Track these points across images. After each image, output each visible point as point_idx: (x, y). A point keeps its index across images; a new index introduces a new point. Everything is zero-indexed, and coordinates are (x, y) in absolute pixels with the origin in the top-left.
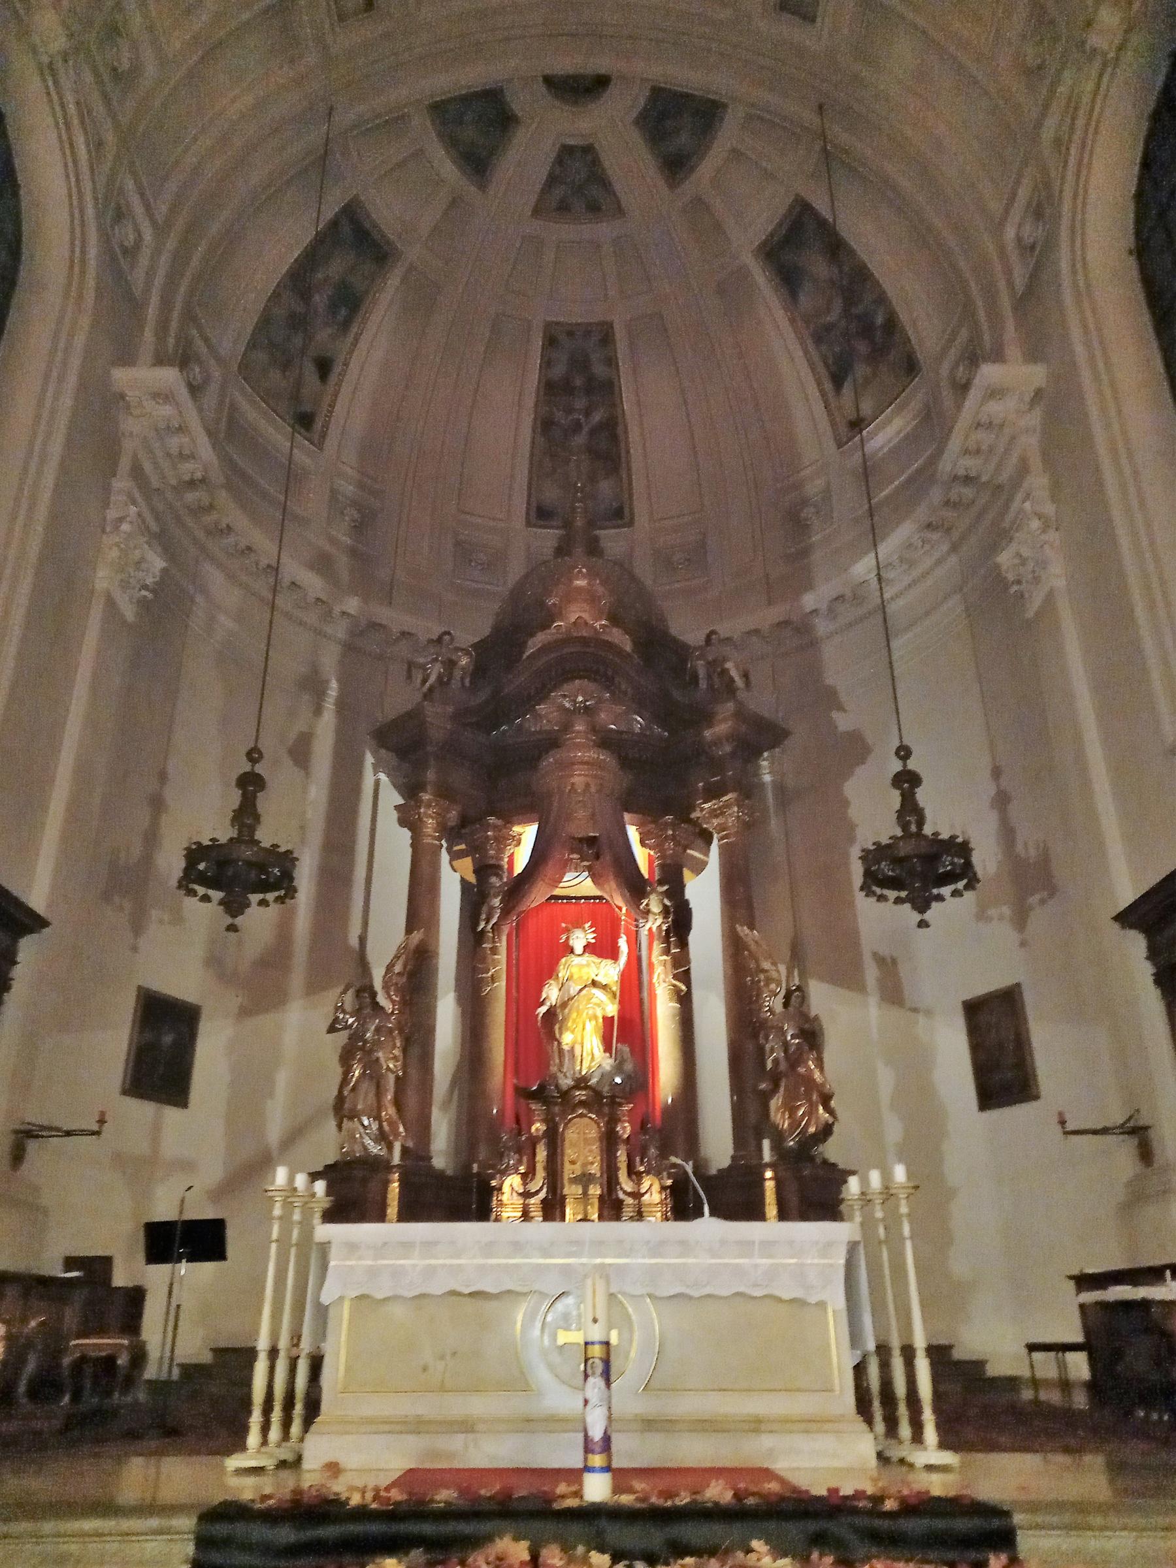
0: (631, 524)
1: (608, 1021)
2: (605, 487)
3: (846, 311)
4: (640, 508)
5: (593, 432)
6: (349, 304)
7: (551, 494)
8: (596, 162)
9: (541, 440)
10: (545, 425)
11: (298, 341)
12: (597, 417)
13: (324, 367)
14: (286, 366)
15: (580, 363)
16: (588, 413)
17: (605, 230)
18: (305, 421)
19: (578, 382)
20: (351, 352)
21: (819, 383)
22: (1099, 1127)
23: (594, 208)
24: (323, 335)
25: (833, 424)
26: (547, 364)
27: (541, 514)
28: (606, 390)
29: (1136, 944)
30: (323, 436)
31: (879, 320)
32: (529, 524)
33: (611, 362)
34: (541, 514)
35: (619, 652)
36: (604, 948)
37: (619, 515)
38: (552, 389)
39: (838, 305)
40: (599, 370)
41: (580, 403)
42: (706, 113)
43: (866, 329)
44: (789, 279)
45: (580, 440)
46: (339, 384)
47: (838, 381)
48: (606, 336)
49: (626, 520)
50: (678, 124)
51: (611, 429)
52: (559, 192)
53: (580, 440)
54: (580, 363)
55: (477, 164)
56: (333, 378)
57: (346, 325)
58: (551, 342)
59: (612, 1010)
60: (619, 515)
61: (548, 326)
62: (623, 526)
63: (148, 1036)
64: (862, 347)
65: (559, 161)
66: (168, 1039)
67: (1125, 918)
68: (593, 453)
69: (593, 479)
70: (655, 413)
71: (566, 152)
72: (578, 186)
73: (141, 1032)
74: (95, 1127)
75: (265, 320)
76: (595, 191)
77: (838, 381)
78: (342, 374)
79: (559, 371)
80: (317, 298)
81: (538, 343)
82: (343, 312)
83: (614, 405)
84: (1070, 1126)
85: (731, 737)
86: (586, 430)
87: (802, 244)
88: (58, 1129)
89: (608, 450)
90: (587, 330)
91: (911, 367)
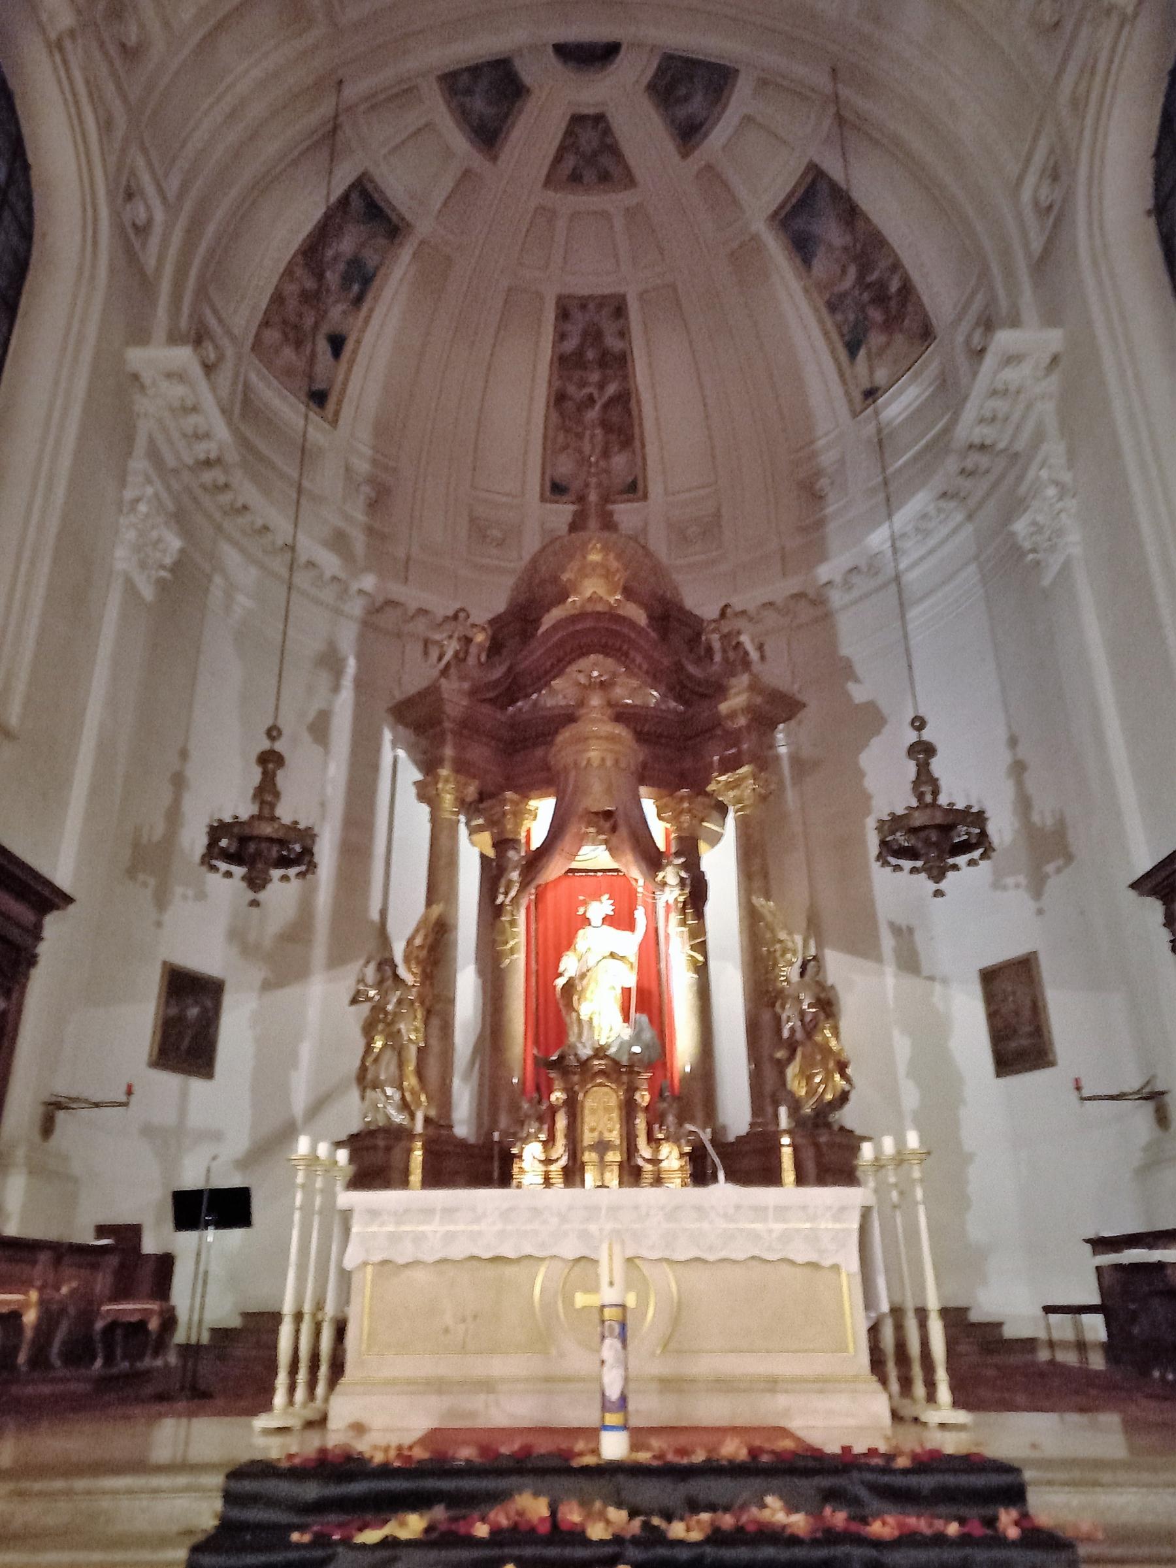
0: (645, 497)
1: (626, 992)
2: (619, 461)
3: (861, 276)
5: (606, 406)
6: (361, 280)
7: (565, 467)
8: (607, 131)
9: (554, 416)
10: (559, 398)
12: (612, 389)
13: (337, 343)
14: (298, 344)
15: (593, 335)
16: (601, 386)
18: (319, 398)
19: (590, 354)
20: (363, 330)
21: (833, 351)
22: (1114, 1092)
23: (605, 177)
24: (336, 311)
25: (847, 393)
26: (561, 336)
27: (557, 489)
28: (618, 363)
29: (1154, 910)
30: (337, 413)
31: (894, 286)
32: (543, 499)
33: (623, 334)
34: (557, 489)
35: (632, 624)
36: (622, 920)
37: (634, 489)
38: (566, 363)
39: (852, 271)
40: (613, 343)
42: (717, 79)
43: (881, 298)
44: (803, 247)
45: (593, 414)
46: (352, 362)
47: (853, 348)
48: (619, 310)
49: (640, 493)
50: (690, 89)
51: (624, 400)
52: (570, 161)
53: (593, 414)
54: (593, 335)
55: (488, 136)
57: (358, 300)
58: (563, 314)
59: (631, 981)
60: (634, 489)
63: (173, 1011)
64: (876, 315)
65: (569, 133)
66: (193, 1012)
67: (1144, 885)
68: (605, 425)
69: (606, 454)
70: (666, 385)
71: (577, 120)
72: (591, 154)
73: (167, 1004)
74: (123, 1099)
75: (278, 298)
76: (606, 160)
77: (853, 348)
78: (355, 352)
79: (570, 345)
80: (328, 274)
81: (550, 315)
82: (356, 288)
84: (1086, 1093)
85: (749, 709)
86: (598, 407)
87: (815, 210)
88: (86, 1101)
89: (621, 424)
90: (602, 301)
91: (926, 334)
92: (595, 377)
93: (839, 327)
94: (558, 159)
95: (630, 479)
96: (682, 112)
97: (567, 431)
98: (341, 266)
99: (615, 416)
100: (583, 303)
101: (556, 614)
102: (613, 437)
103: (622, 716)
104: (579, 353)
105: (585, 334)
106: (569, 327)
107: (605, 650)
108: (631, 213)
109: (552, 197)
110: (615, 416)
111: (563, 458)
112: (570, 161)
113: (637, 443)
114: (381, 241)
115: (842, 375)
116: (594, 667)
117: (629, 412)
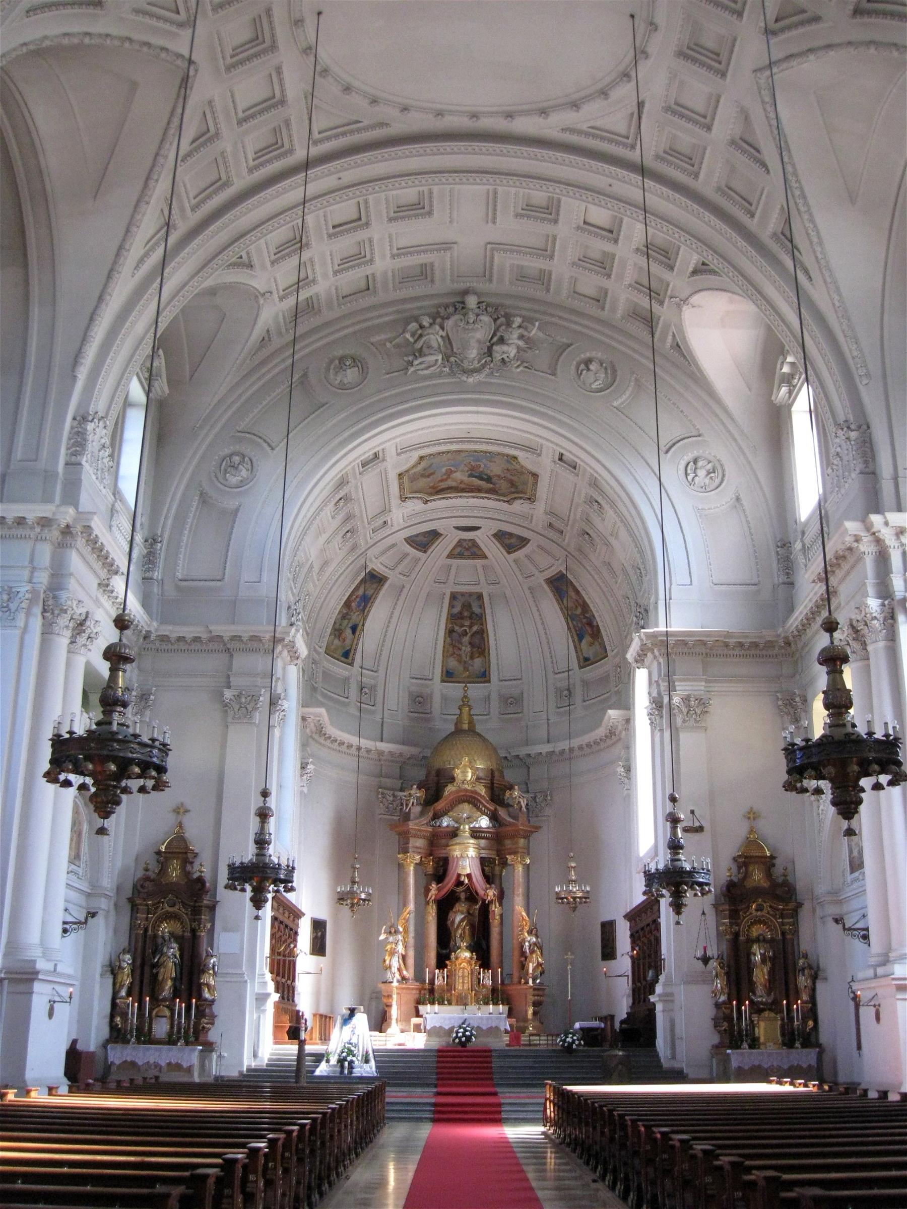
0: (489, 681)
2: (478, 662)
4: (494, 677)
5: (472, 635)
7: (453, 663)
10: (450, 632)
11: (346, 622)
12: (475, 628)
13: (354, 629)
15: (467, 606)
16: (470, 627)
17: (479, 562)
18: (347, 656)
19: (466, 614)
24: (355, 617)
25: (578, 657)
26: (451, 606)
27: (448, 676)
30: (353, 659)
32: (443, 681)
33: (482, 606)
34: (448, 676)
37: (484, 676)
38: (454, 618)
40: (477, 610)
43: (590, 624)
45: (466, 639)
47: (581, 637)
48: (480, 596)
50: (510, 542)
51: (482, 633)
53: (466, 639)
54: (467, 606)
56: (357, 633)
58: (454, 597)
60: (484, 676)
61: (452, 593)
62: (484, 682)
66: (320, 934)
69: (472, 658)
72: (468, 550)
75: (335, 623)
76: (475, 550)
77: (581, 637)
79: (456, 610)
83: (482, 624)
90: (471, 594)
92: (467, 623)
93: (574, 626)
94: (454, 548)
95: (483, 670)
96: (507, 541)
97: (454, 646)
98: (358, 600)
99: (477, 641)
100: (463, 594)
101: (450, 789)
102: (475, 649)
103: (476, 834)
104: (461, 613)
105: (463, 606)
106: (455, 603)
107: (469, 802)
108: (484, 567)
109: (450, 561)
111: (451, 659)
112: (458, 550)
113: (486, 655)
114: (375, 586)
115: (575, 647)
116: (465, 810)
117: (483, 638)
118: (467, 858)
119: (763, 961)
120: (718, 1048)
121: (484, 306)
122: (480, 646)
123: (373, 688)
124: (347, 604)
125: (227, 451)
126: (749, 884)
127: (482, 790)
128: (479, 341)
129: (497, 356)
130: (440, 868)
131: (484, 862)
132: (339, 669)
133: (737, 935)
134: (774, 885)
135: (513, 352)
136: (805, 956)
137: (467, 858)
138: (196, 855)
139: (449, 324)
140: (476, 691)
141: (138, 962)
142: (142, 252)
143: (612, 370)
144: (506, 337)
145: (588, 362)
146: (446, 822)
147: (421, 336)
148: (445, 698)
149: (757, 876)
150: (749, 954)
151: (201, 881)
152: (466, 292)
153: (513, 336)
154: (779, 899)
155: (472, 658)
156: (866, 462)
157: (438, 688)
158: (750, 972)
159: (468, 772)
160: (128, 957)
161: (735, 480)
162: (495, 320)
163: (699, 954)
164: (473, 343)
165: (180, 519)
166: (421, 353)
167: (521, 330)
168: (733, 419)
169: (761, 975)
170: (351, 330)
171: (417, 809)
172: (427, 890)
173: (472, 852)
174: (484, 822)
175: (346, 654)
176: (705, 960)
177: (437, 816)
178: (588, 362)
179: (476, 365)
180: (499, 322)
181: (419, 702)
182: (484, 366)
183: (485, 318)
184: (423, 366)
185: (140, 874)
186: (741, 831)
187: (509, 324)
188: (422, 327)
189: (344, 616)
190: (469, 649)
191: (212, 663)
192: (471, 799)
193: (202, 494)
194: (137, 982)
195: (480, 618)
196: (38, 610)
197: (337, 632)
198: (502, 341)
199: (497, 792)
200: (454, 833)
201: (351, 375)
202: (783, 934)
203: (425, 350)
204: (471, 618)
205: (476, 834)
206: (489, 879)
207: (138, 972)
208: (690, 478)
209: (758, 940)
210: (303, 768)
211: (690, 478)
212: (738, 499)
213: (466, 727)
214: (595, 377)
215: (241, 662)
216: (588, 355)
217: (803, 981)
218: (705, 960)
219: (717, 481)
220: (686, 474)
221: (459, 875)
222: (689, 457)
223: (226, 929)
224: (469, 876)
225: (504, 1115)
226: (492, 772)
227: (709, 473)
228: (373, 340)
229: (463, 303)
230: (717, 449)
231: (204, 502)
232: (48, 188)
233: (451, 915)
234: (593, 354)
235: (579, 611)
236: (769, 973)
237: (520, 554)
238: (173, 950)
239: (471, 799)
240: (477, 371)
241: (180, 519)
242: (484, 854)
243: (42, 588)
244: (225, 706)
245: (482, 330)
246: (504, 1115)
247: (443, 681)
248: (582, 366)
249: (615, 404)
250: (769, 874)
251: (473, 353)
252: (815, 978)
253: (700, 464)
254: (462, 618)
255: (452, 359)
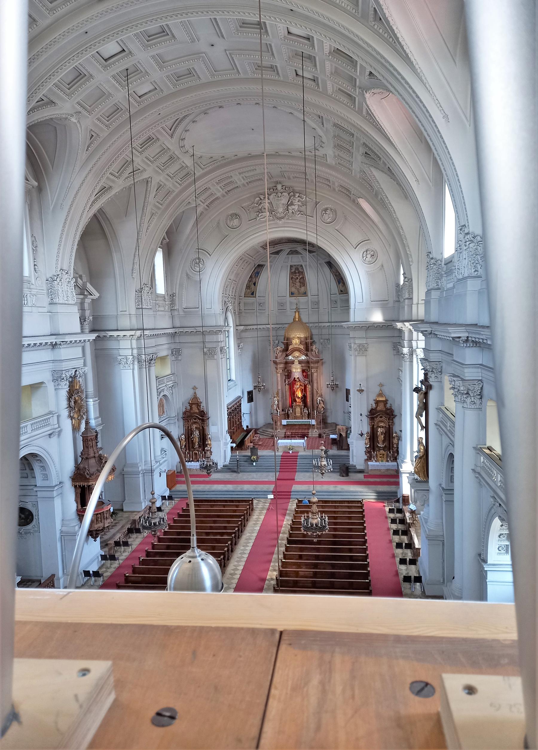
2: (303, 288)
7: (293, 290)
9: (291, 281)
12: (301, 277)
13: (254, 284)
16: (299, 276)
17: (300, 256)
32: (290, 297)
33: (303, 269)
34: (292, 294)
37: (305, 294)
38: (291, 273)
40: (300, 270)
41: (298, 275)
45: (298, 280)
48: (301, 266)
51: (303, 278)
53: (298, 280)
58: (291, 266)
60: (305, 294)
69: (300, 287)
70: (311, 276)
79: (293, 271)
92: (298, 275)
101: (290, 347)
103: (300, 362)
104: (295, 271)
110: (302, 280)
116: (297, 354)
118: (297, 371)
119: (382, 434)
120: (366, 460)
121: (285, 188)
122: (303, 282)
123: (264, 303)
124: (251, 277)
125: (194, 258)
126: (379, 408)
127: (302, 347)
128: (283, 204)
129: (290, 211)
130: (288, 374)
131: (303, 371)
132: (251, 300)
133: (373, 425)
134: (387, 409)
135: (296, 207)
136: (396, 433)
137: (297, 371)
138: (201, 403)
139: (271, 197)
140: (302, 299)
141: (187, 437)
142: (147, 226)
143: (334, 211)
144: (294, 201)
145: (326, 210)
146: (290, 357)
147: (261, 203)
148: (291, 303)
149: (381, 407)
150: (377, 431)
151: (203, 411)
152: (277, 183)
153: (296, 202)
154: (387, 414)
155: (300, 287)
156: (409, 294)
157: (288, 299)
158: (377, 437)
159: (297, 337)
160: (183, 436)
161: (382, 258)
162: (289, 194)
163: (360, 433)
164: (281, 205)
165: (181, 285)
166: (260, 211)
167: (299, 198)
168: (381, 232)
169: (381, 438)
170: (234, 202)
171: (281, 353)
172: (285, 382)
173: (299, 370)
174: (303, 357)
175: (252, 294)
176: (362, 435)
177: (287, 356)
178: (326, 210)
179: (282, 215)
180: (290, 194)
181: (281, 305)
182: (285, 215)
183: (284, 194)
184: (262, 217)
185: (184, 410)
186: (377, 390)
187: (294, 196)
188: (261, 199)
189: (250, 281)
190: (299, 284)
191: (199, 338)
192: (299, 350)
193: (187, 275)
194: (187, 442)
195: (302, 273)
196: (136, 363)
197: (248, 287)
198: (292, 204)
199: (307, 347)
200: (293, 362)
201: (236, 222)
202: (389, 425)
203: (263, 210)
204: (299, 273)
205: (300, 362)
206: (306, 377)
207: (187, 440)
208: (364, 258)
209: (380, 427)
210: (238, 347)
211: (364, 258)
212: (382, 266)
213: (297, 320)
214: (328, 217)
215: (208, 338)
216: (326, 206)
217: (395, 441)
218: (362, 435)
219: (375, 259)
220: (363, 257)
221: (295, 378)
222: (365, 249)
223: (213, 425)
224: (298, 378)
225: (291, 497)
226: (306, 338)
227: (372, 256)
228: (242, 206)
229: (276, 186)
230: (376, 245)
231: (188, 278)
232: (108, 216)
233: (295, 386)
234: (328, 206)
235: (338, 274)
236: (384, 437)
237: (314, 254)
238: (197, 433)
239: (299, 350)
240: (283, 218)
241: (181, 285)
242: (304, 368)
243: (136, 355)
244: (205, 354)
245: (284, 200)
246: (291, 497)
247: (290, 297)
248: (324, 212)
249: (336, 228)
250: (385, 406)
251: (281, 210)
252: (398, 440)
253: (368, 252)
254: (296, 273)
255: (273, 213)
